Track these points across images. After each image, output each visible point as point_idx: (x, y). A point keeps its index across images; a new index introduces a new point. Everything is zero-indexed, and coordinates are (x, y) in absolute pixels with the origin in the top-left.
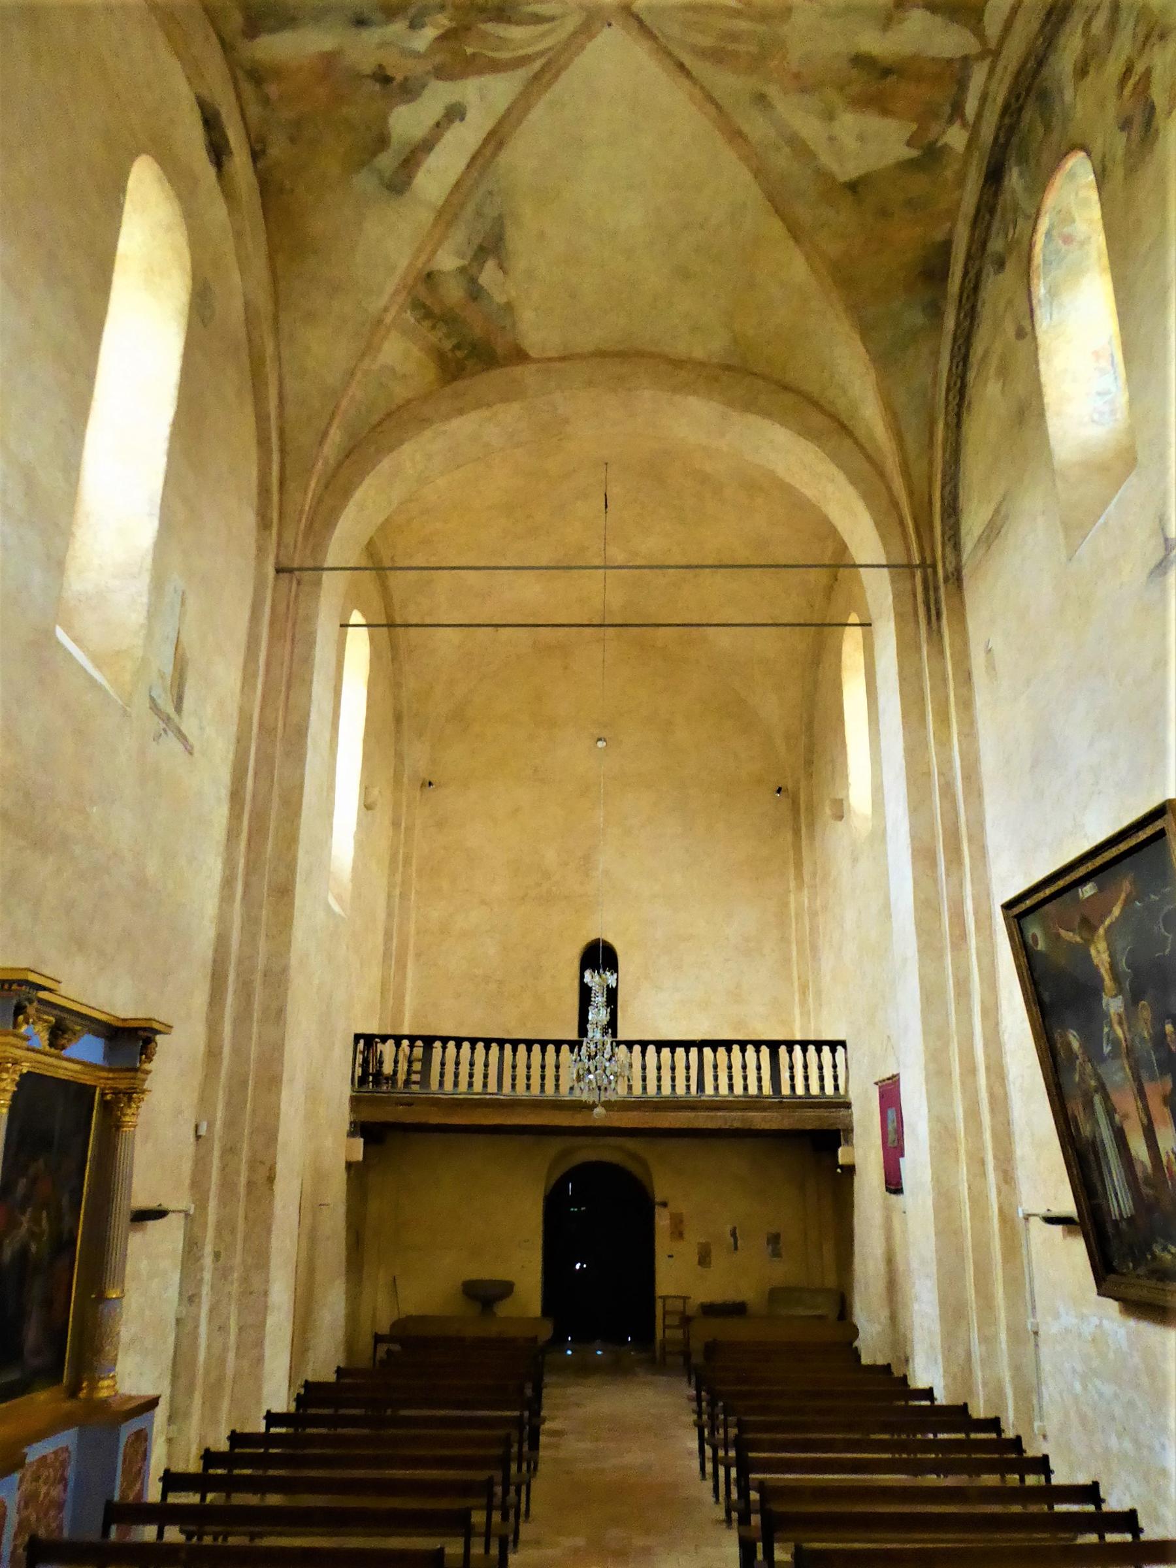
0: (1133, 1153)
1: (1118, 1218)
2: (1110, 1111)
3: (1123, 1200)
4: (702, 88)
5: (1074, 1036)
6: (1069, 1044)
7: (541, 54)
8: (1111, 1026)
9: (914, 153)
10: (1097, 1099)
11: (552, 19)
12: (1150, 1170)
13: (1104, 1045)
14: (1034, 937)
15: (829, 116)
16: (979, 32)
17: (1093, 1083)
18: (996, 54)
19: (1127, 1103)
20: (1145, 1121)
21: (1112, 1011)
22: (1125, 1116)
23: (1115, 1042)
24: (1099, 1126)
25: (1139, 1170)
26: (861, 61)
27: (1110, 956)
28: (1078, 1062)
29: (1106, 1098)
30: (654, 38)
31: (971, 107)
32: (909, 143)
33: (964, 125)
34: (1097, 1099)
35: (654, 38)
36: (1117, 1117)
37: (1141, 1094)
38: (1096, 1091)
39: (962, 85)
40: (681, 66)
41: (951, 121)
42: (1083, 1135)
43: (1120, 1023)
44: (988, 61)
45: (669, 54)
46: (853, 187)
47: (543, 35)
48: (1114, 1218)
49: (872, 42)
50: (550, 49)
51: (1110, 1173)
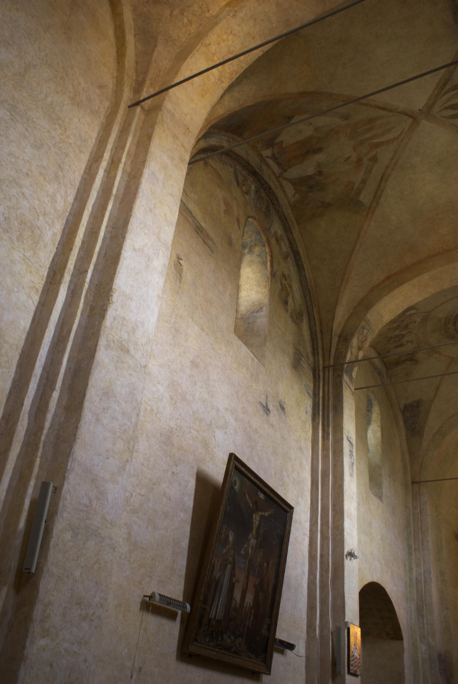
0: (234, 596)
1: (212, 617)
2: (233, 575)
3: (219, 612)
4: (371, 106)
5: (232, 535)
6: (227, 537)
7: (447, 92)
8: (248, 547)
9: (277, 140)
10: (229, 566)
11: (447, 108)
12: (238, 605)
14: (235, 480)
15: (316, 129)
16: (287, 179)
18: (277, 178)
19: (240, 576)
20: (245, 587)
21: (251, 542)
22: (238, 581)
23: (247, 553)
24: (224, 577)
26: (320, 150)
27: (259, 524)
28: (228, 546)
29: (233, 569)
30: (399, 113)
31: (270, 162)
32: (282, 142)
33: (268, 157)
34: (229, 566)
35: (399, 113)
36: (234, 579)
37: (247, 577)
38: (231, 563)
39: (279, 164)
40: (384, 109)
41: (273, 155)
42: (214, 575)
43: (252, 549)
44: (277, 175)
45: (390, 111)
46: (290, 118)
47: (448, 101)
48: (210, 617)
49: (320, 157)
50: (444, 95)
51: (219, 598)
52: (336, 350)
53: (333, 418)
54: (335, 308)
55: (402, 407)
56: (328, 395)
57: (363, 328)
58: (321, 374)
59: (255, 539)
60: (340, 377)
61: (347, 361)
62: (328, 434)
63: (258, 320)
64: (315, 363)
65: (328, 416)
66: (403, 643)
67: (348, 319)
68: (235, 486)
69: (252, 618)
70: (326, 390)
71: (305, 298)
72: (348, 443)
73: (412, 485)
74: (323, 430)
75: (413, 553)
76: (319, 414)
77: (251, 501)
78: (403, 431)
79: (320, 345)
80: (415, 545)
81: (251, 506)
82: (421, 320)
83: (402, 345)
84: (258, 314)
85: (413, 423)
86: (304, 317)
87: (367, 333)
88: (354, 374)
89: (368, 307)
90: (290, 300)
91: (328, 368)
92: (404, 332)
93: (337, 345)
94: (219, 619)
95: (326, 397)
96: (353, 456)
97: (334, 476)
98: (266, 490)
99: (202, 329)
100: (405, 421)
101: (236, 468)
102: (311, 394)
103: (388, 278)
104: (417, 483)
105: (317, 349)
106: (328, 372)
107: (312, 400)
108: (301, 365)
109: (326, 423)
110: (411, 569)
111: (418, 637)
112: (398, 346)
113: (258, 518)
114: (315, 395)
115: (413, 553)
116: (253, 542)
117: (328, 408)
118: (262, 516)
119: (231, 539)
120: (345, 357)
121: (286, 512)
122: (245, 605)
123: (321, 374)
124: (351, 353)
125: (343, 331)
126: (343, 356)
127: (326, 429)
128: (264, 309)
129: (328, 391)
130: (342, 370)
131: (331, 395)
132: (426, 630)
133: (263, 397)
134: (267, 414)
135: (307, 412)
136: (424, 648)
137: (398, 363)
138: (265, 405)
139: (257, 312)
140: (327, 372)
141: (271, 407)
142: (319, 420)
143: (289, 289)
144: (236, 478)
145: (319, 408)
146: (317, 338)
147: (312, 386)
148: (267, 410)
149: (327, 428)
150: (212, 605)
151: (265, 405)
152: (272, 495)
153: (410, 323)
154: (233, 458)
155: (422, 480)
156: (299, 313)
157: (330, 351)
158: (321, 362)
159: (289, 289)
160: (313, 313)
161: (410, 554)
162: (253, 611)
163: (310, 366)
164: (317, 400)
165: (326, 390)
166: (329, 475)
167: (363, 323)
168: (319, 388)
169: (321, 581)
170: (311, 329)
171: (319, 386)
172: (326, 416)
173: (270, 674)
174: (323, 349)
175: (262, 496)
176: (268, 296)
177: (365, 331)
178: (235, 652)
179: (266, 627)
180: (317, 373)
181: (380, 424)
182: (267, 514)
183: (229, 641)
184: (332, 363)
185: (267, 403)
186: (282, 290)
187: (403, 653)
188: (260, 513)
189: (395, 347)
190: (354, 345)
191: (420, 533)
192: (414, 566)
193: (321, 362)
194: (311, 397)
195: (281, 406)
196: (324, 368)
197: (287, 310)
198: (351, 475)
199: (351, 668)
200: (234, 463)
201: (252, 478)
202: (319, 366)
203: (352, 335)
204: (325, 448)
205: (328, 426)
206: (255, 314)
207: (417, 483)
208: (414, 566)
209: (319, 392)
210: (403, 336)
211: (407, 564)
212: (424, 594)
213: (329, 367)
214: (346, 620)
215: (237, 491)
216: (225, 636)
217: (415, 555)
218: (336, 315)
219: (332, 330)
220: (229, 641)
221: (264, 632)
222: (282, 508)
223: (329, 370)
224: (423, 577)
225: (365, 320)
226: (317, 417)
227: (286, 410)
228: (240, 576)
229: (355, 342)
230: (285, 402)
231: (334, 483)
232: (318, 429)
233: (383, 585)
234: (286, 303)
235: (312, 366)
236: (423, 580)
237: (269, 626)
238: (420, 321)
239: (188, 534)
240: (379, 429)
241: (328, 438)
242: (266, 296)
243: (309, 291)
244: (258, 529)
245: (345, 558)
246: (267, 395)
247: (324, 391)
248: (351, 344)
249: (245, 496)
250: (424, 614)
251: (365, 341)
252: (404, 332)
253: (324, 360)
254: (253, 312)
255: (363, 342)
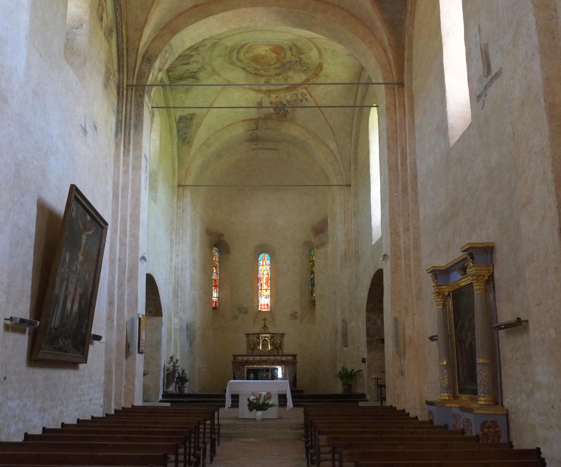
0: (67, 307)
2: (67, 289)
6: (65, 257)
10: (65, 282)
12: (68, 314)
13: (74, 266)
14: (73, 208)
17: (66, 276)
20: (74, 298)
22: (70, 294)
23: (77, 268)
25: (66, 312)
27: (85, 242)
28: (65, 266)
29: (67, 284)
34: (65, 282)
36: (68, 292)
37: (76, 289)
38: (66, 279)
43: (80, 265)
48: (51, 327)
52: (139, 69)
53: (133, 136)
54: (143, 28)
55: (177, 118)
56: (130, 113)
57: (166, 51)
58: (125, 91)
59: (82, 255)
60: (142, 96)
61: (148, 84)
62: (129, 151)
63: (78, 38)
64: (119, 81)
65: (129, 134)
66: (161, 320)
67: (153, 40)
68: (73, 213)
69: (76, 322)
70: (128, 108)
71: (116, 12)
72: (145, 159)
73: (178, 188)
74: (124, 147)
75: (174, 245)
76: (121, 132)
77: (82, 223)
78: (176, 139)
79: (125, 63)
80: (176, 239)
81: (82, 228)
82: (211, 45)
83: (188, 63)
84: (78, 30)
85: (185, 134)
86: (114, 33)
87: (168, 56)
88: (152, 94)
89: (174, 33)
90: (105, 16)
91: (131, 87)
92: (194, 53)
93: (141, 64)
94: (56, 327)
95: (128, 115)
96: (147, 171)
97: (133, 190)
98: (92, 212)
99: (41, 56)
100: (178, 131)
101: (76, 198)
102: (115, 111)
103: (196, 6)
104: (182, 186)
105: (123, 67)
106: (131, 91)
107: (115, 117)
108: (110, 83)
109: (127, 140)
110: (171, 259)
111: (173, 313)
112: (185, 64)
113: (85, 238)
114: (119, 112)
115: (174, 245)
116: (81, 258)
117: (130, 126)
118: (88, 235)
119: (67, 259)
120: (148, 78)
121: (103, 228)
122: (73, 311)
123: (125, 91)
124: (153, 74)
125: (147, 51)
126: (146, 76)
127: (127, 146)
128: (84, 26)
129: (131, 110)
130: (144, 91)
131: (133, 114)
132: (179, 307)
133: (83, 119)
134: (85, 135)
135: (111, 130)
136: (176, 320)
137: (181, 78)
138: (84, 127)
139: (77, 28)
140: (130, 91)
141: (88, 129)
142: (121, 137)
143: (104, 4)
144: (74, 206)
145: (121, 125)
146: (123, 56)
147: (116, 103)
148: (85, 131)
149: (128, 145)
150: (52, 317)
151: (84, 127)
152: (95, 216)
153: (201, 46)
154: (74, 189)
155: (187, 184)
156: (110, 28)
157: (134, 70)
158: (125, 80)
159: (104, 4)
160: (122, 29)
161: (172, 246)
162: (78, 316)
163: (116, 84)
164: (120, 118)
165: (128, 108)
166: (128, 189)
167: (167, 47)
168: (122, 106)
169: (119, 281)
170: (118, 46)
171: (123, 104)
172: (127, 133)
173: (87, 363)
174: (127, 67)
175: (88, 217)
176: (89, 13)
177: (167, 55)
178: (66, 351)
179: (85, 327)
180: (121, 90)
181: (159, 134)
182: (90, 233)
183: (62, 343)
184: (135, 83)
185: (85, 125)
186: (99, 5)
187: (162, 326)
188: (87, 233)
189: (182, 64)
190: (156, 67)
191: (181, 230)
192: (174, 255)
193: (125, 80)
194: (115, 114)
195: (95, 127)
196: (127, 86)
197: (102, 27)
198: (145, 189)
199: (141, 348)
200: (74, 194)
201: (84, 203)
202: (123, 84)
203: (156, 57)
204: (126, 164)
205: (129, 143)
206: (74, 30)
207: (182, 186)
208: (174, 255)
209: (122, 110)
210: (192, 56)
211: (169, 255)
212: (180, 279)
213: (132, 86)
214: (138, 312)
215: (74, 216)
216: (60, 340)
217: (176, 248)
218: (143, 36)
219: (138, 50)
220: (62, 343)
221: (84, 330)
222: (99, 223)
223: (132, 89)
224: (180, 265)
225: (169, 45)
226: (120, 134)
227: (98, 129)
228: (71, 289)
229: (157, 64)
230: (97, 122)
231: (133, 195)
232: (120, 146)
233: (153, 276)
234: (101, 19)
235: (117, 83)
236: (180, 268)
237: (87, 325)
238: (210, 45)
239: (32, 257)
240: (158, 138)
241: (128, 155)
242: (87, 12)
243: (120, 6)
244: (85, 246)
245: (139, 261)
246: (85, 117)
247: (126, 110)
248: (154, 66)
249: (78, 219)
250: (179, 295)
251: (165, 63)
252: (194, 53)
253: (128, 79)
254: (73, 28)
255: (163, 64)
